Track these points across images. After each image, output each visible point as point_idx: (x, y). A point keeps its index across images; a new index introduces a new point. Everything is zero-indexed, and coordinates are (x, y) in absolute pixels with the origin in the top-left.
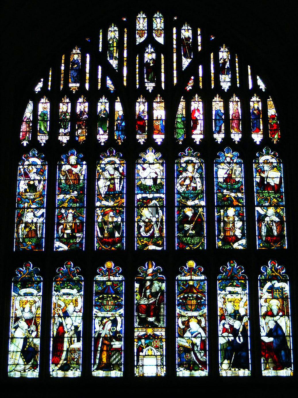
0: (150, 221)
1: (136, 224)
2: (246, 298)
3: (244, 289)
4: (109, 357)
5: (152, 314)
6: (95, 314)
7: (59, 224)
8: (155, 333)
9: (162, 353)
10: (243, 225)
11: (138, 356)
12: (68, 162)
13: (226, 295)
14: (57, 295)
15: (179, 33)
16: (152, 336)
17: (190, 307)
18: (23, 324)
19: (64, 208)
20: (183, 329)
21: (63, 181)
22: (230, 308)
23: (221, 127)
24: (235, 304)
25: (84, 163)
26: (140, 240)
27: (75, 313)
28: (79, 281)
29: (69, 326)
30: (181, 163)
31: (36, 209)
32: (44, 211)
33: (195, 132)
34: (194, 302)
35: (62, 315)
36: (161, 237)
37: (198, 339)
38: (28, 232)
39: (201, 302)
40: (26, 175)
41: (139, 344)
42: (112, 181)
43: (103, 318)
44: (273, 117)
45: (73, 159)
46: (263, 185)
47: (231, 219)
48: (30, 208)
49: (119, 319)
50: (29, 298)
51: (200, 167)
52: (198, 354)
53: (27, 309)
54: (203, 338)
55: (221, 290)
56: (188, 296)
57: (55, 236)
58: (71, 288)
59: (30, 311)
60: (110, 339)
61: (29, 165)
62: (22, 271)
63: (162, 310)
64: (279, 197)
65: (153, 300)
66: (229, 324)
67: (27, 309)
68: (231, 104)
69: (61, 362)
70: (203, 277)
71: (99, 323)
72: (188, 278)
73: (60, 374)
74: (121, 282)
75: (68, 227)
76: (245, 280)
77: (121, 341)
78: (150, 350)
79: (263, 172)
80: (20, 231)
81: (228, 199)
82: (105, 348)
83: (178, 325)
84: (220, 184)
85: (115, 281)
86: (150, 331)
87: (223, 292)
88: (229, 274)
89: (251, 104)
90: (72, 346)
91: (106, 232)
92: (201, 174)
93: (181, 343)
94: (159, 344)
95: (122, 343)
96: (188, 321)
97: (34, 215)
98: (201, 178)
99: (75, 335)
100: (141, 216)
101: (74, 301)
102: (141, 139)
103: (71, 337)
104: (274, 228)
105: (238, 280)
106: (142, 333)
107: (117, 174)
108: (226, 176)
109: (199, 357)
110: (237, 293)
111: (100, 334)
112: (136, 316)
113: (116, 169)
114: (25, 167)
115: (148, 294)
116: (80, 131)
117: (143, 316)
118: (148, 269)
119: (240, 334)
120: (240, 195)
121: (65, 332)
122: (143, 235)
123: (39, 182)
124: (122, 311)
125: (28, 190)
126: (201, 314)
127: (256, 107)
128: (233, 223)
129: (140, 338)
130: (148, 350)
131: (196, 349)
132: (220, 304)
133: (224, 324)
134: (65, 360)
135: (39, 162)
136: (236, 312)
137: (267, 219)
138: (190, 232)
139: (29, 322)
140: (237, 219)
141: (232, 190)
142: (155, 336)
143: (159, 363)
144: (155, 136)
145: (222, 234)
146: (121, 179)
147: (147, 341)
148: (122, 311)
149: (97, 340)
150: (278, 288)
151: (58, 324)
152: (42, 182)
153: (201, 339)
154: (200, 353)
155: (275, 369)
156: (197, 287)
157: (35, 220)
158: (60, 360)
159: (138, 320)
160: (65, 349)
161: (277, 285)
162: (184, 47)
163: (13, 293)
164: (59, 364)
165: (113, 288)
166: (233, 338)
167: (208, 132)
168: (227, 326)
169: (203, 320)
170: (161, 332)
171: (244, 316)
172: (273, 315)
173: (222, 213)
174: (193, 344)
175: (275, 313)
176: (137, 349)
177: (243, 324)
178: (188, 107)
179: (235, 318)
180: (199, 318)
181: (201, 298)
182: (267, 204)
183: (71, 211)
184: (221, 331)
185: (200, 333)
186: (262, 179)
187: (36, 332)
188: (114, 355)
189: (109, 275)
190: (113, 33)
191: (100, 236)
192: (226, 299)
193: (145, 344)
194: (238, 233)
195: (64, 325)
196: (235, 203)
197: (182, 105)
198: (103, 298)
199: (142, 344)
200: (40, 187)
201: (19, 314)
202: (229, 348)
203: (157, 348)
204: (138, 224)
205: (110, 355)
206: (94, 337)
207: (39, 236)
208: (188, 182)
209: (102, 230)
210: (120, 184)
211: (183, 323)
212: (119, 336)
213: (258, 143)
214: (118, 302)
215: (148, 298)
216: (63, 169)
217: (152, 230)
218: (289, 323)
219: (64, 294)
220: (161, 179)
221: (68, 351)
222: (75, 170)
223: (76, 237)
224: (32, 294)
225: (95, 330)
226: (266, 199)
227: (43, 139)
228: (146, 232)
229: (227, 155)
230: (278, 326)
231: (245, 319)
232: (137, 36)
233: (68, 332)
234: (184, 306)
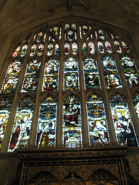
0: (71, 81)
1: (64, 82)
2: (127, 110)
3: (125, 106)
5: (73, 120)
6: (39, 121)
7: (25, 83)
8: (75, 129)
9: (80, 141)
10: (119, 80)
12: (33, 62)
13: (116, 109)
14: (19, 113)
16: (73, 131)
17: (95, 116)
19: (28, 77)
20: (93, 127)
22: (119, 115)
24: (122, 113)
25: (40, 62)
26: (66, 88)
27: (28, 121)
29: (23, 128)
30: (85, 61)
31: (15, 78)
34: (98, 113)
35: (20, 122)
36: (77, 86)
37: (102, 131)
38: (9, 87)
39: (102, 113)
40: (13, 67)
41: (65, 136)
43: (44, 123)
48: (12, 78)
49: (53, 123)
54: (105, 131)
55: (113, 107)
56: (94, 111)
57: (22, 88)
60: (48, 133)
61: (14, 64)
62: (1, 102)
63: (79, 118)
65: (73, 114)
66: (120, 123)
69: (15, 148)
70: (101, 102)
71: (41, 125)
72: (93, 102)
74: (56, 105)
75: (29, 84)
76: (125, 102)
77: (54, 134)
78: (72, 139)
79: (125, 62)
81: (110, 72)
82: (44, 139)
83: (89, 125)
85: (52, 105)
86: (72, 129)
87: (114, 108)
88: (116, 100)
90: (24, 138)
91: (48, 85)
93: (92, 134)
95: (55, 135)
96: (95, 123)
97: (13, 81)
99: (26, 132)
101: (28, 115)
103: (24, 133)
105: (121, 102)
106: (67, 130)
108: (107, 64)
111: (41, 131)
112: (64, 121)
115: (70, 111)
116: (39, 53)
117: (68, 121)
118: (70, 99)
119: (128, 128)
120: (115, 70)
121: (20, 131)
122: (67, 86)
123: (18, 69)
124: (55, 119)
125: (12, 72)
126: (102, 119)
127: (117, 44)
128: (114, 79)
129: (66, 133)
130: (71, 139)
131: (101, 137)
132: (113, 113)
134: (18, 146)
135: (19, 63)
138: (92, 84)
140: (115, 78)
141: (111, 68)
142: (75, 132)
146: (57, 67)
147: (71, 134)
148: (55, 119)
149: (39, 135)
151: (17, 127)
153: (104, 132)
154: (105, 139)
156: (99, 106)
157: (13, 82)
158: (15, 147)
159: (65, 123)
160: (19, 140)
164: (14, 149)
165: (51, 109)
166: (124, 130)
169: (104, 121)
170: (79, 129)
171: (128, 119)
174: (100, 135)
176: (64, 139)
177: (128, 123)
178: (87, 45)
179: (123, 120)
180: (101, 121)
181: (102, 111)
182: (129, 73)
183: (32, 78)
184: (116, 127)
185: (103, 128)
186: (125, 65)
187: (3, 131)
188: (49, 142)
189: (49, 103)
191: (45, 87)
192: (116, 111)
193: (69, 136)
194: (117, 83)
195: (21, 127)
196: (114, 73)
198: (44, 113)
199: (67, 136)
202: (122, 136)
203: (77, 137)
204: (65, 82)
205: (47, 143)
206: (38, 133)
208: (89, 67)
209: (46, 85)
210: (56, 68)
211: (92, 124)
212: (53, 132)
214: (53, 115)
215: (71, 112)
216: (30, 65)
217: (72, 84)
219: (23, 112)
220: (76, 66)
223: (33, 88)
224: (5, 113)
225: (39, 129)
226: (129, 71)
228: (69, 85)
231: (129, 121)
233: (22, 130)
234: (92, 115)
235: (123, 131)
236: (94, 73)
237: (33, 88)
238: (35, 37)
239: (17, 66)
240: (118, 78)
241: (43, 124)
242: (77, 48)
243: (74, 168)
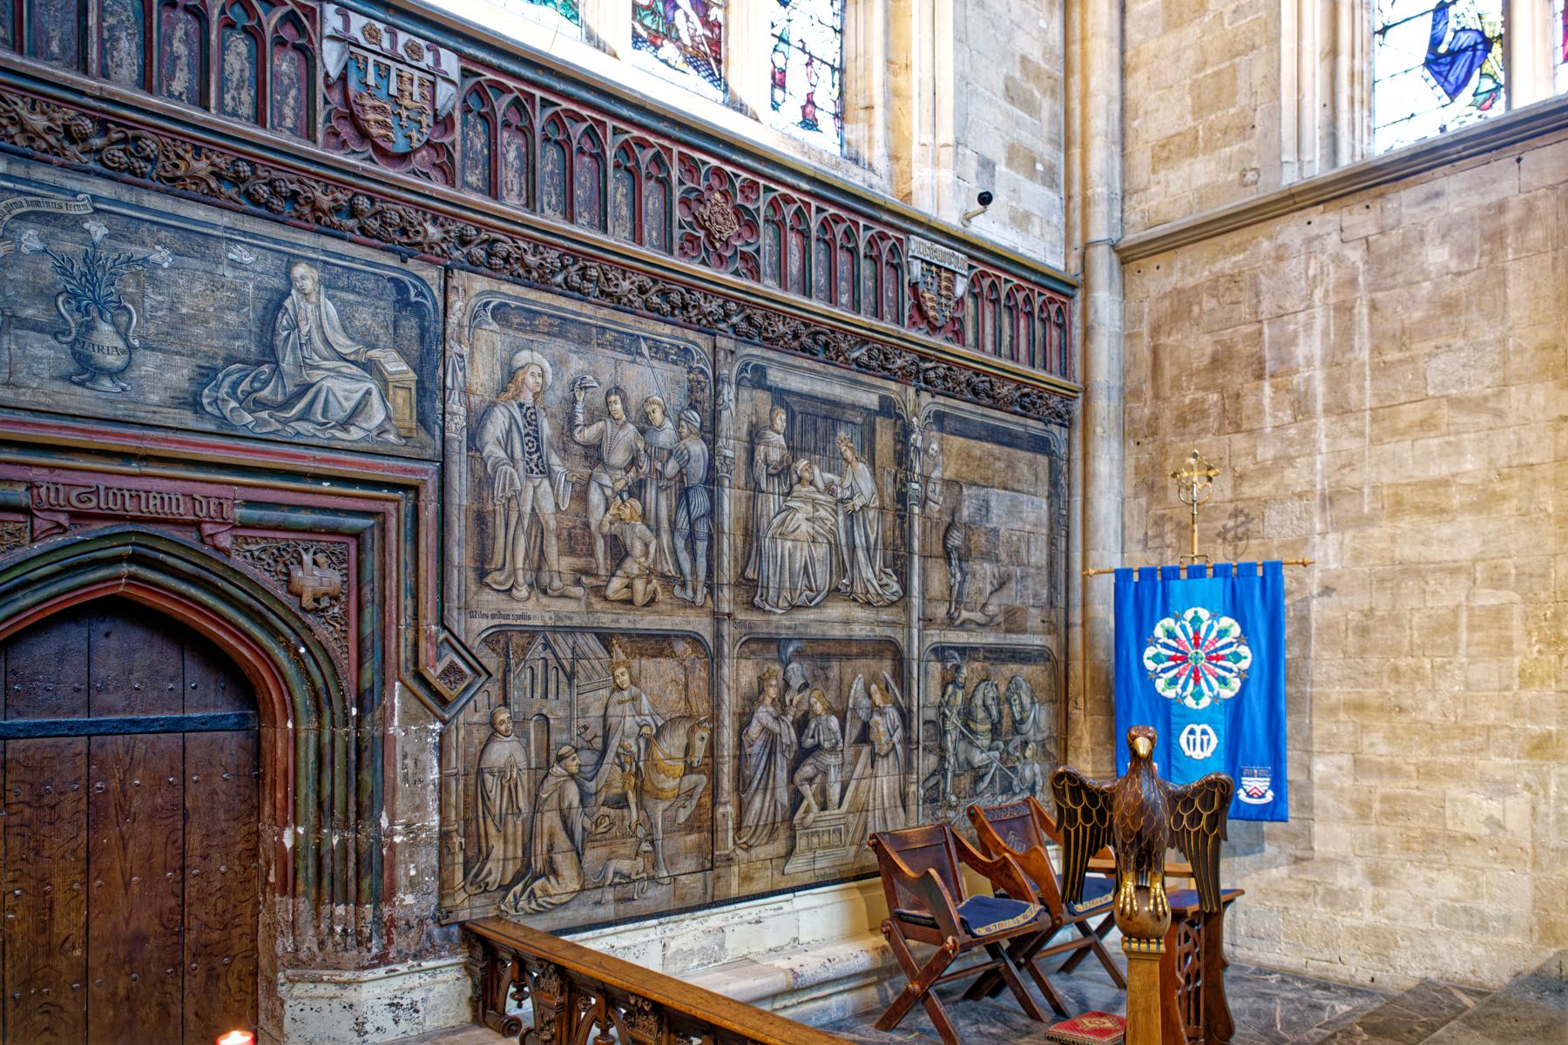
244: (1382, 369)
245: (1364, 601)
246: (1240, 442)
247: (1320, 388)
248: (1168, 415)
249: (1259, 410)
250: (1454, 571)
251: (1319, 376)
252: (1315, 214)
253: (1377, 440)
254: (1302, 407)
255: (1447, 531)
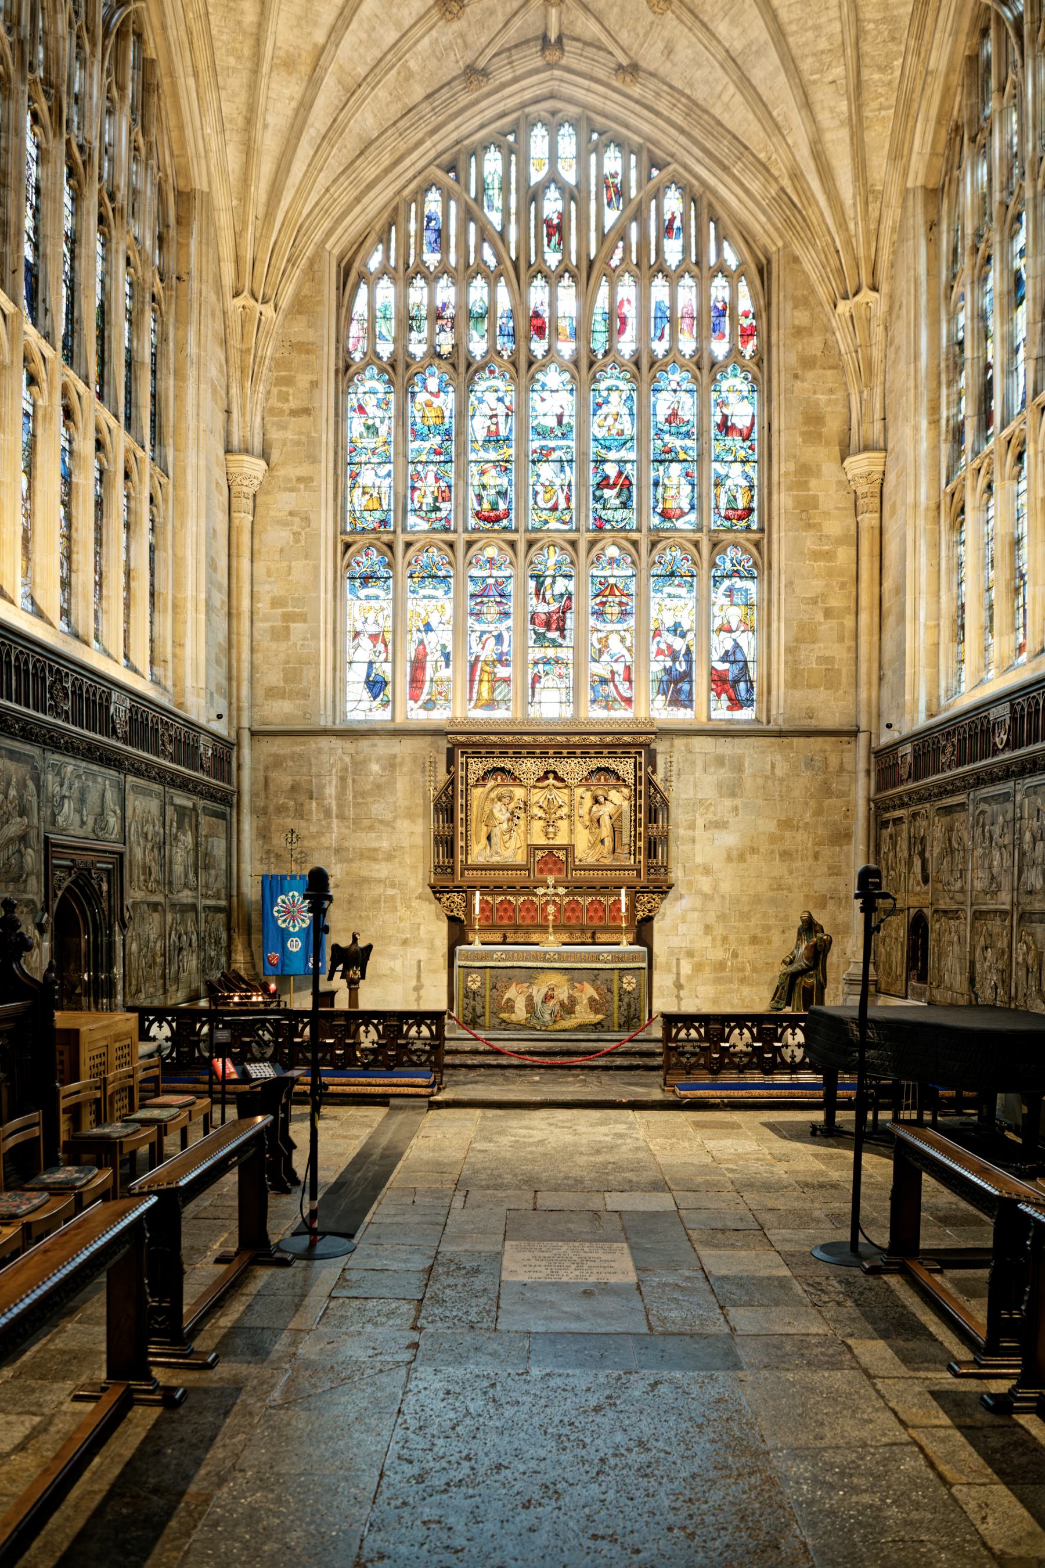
0: (552, 485)
2: (692, 603)
4: (493, 690)
7: (414, 489)
11: (533, 688)
13: (663, 599)
15: (600, 165)
18: (365, 642)
21: (418, 420)
23: (663, 330)
25: (451, 389)
28: (445, 577)
29: (433, 645)
32: (389, 467)
33: (623, 338)
34: (617, 609)
40: (361, 409)
42: (494, 420)
43: (483, 633)
44: (746, 315)
45: (433, 384)
46: (726, 427)
47: (675, 480)
49: (506, 635)
50: (373, 603)
51: (630, 398)
52: (620, 687)
53: (371, 620)
55: (658, 591)
58: (434, 588)
59: (376, 622)
64: (750, 448)
67: (371, 620)
68: (680, 289)
72: (607, 573)
73: (423, 715)
80: (355, 500)
84: (660, 426)
86: (551, 653)
87: (659, 595)
89: (713, 290)
92: (631, 409)
94: (563, 671)
96: (607, 638)
98: (631, 414)
100: (538, 476)
102: (539, 347)
104: (739, 496)
106: (538, 656)
107: (501, 410)
108: (670, 412)
109: (622, 691)
110: (679, 597)
113: (500, 400)
114: (360, 396)
117: (542, 630)
119: (681, 658)
121: (425, 655)
124: (510, 622)
129: (536, 663)
132: (653, 614)
133: (658, 643)
135: (380, 387)
136: (677, 626)
137: (729, 483)
139: (374, 637)
140: (683, 481)
143: (564, 699)
144: (560, 345)
145: (661, 506)
146: (507, 415)
147: (547, 668)
150: (739, 589)
152: (387, 421)
155: (729, 708)
157: (378, 483)
160: (428, 678)
161: (738, 583)
162: (608, 187)
163: (349, 596)
167: (643, 336)
168: (663, 646)
172: (730, 631)
173: (661, 473)
174: (613, 673)
175: (734, 628)
180: (622, 633)
182: (731, 458)
186: (725, 417)
190: (493, 163)
195: (426, 642)
196: (682, 456)
197: (604, 291)
200: (383, 430)
201: (359, 627)
203: (560, 676)
207: (385, 507)
208: (610, 421)
209: (480, 498)
211: (600, 641)
213: (721, 358)
218: (753, 643)
219: (424, 597)
221: (432, 680)
222: (437, 402)
223: (439, 509)
224: (377, 598)
227: (385, 349)
228: (547, 502)
229: (671, 377)
230: (737, 646)
232: (532, 169)
235: (668, 664)
236: (623, 454)
237: (439, 509)
238: (413, 227)
239: (375, 402)
240: (693, 485)
241: (480, 637)
242: (574, 314)
243: (552, 764)
244: (356, 805)
245: (349, 890)
246: (303, 824)
247: (334, 808)
248: (271, 809)
249: (310, 812)
250: (380, 881)
251: (334, 803)
252: (333, 739)
253: (354, 831)
254: (328, 813)
255: (377, 867)
